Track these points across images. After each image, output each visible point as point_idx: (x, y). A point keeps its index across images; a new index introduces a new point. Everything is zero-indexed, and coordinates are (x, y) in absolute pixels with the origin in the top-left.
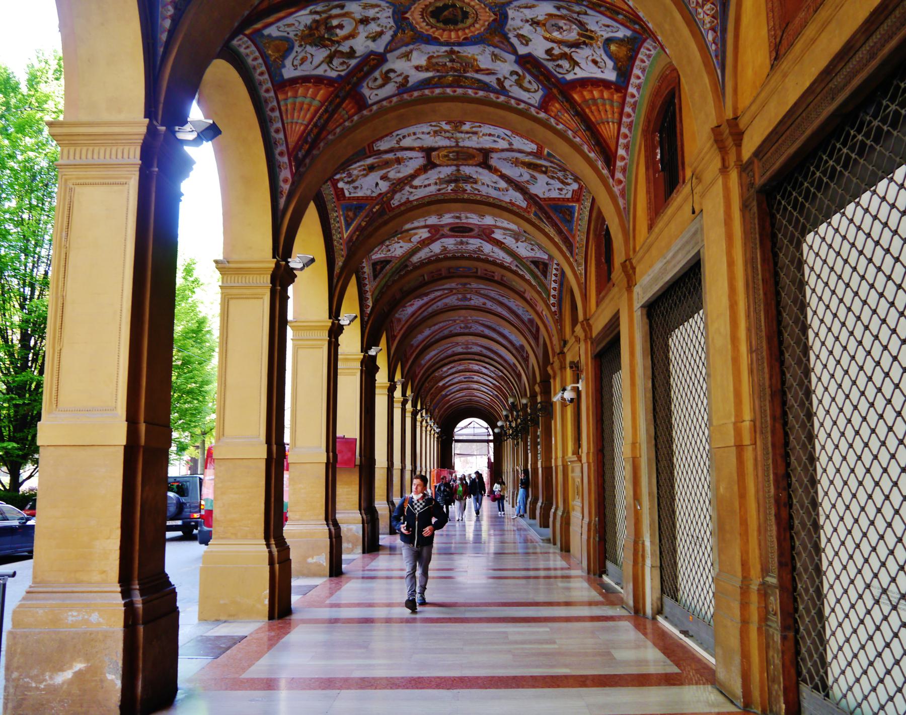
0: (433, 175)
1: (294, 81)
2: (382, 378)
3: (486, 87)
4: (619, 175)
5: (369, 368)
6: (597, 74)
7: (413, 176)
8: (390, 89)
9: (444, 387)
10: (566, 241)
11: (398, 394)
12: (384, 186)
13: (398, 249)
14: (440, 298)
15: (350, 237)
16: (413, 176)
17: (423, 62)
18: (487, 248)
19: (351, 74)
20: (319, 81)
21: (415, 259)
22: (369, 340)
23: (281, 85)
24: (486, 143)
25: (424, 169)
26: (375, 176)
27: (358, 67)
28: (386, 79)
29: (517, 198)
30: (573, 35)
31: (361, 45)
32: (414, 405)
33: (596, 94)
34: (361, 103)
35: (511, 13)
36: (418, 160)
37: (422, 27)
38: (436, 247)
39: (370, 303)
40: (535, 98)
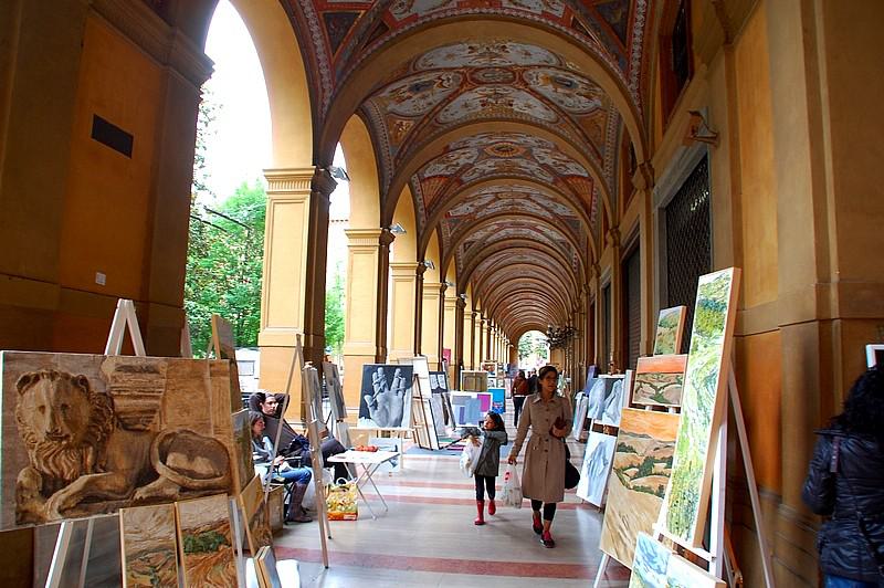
0: (499, 203)
1: (429, 178)
2: (468, 309)
3: (525, 173)
4: (593, 219)
5: (460, 306)
6: (579, 173)
7: (488, 204)
8: (476, 175)
9: (511, 310)
10: (578, 241)
11: (478, 318)
12: (472, 210)
13: (479, 235)
14: (506, 257)
15: (452, 237)
16: (488, 204)
17: (492, 164)
18: (534, 233)
19: (457, 172)
20: (441, 176)
21: (489, 240)
22: (460, 291)
23: (423, 180)
24: (527, 191)
25: (494, 201)
26: (466, 206)
27: (460, 170)
28: (474, 172)
29: (548, 214)
30: (565, 158)
31: (462, 161)
32: (489, 324)
33: (579, 181)
34: (461, 182)
35: (534, 149)
36: (492, 197)
37: (492, 153)
38: (502, 233)
39: (462, 266)
40: (551, 179)
